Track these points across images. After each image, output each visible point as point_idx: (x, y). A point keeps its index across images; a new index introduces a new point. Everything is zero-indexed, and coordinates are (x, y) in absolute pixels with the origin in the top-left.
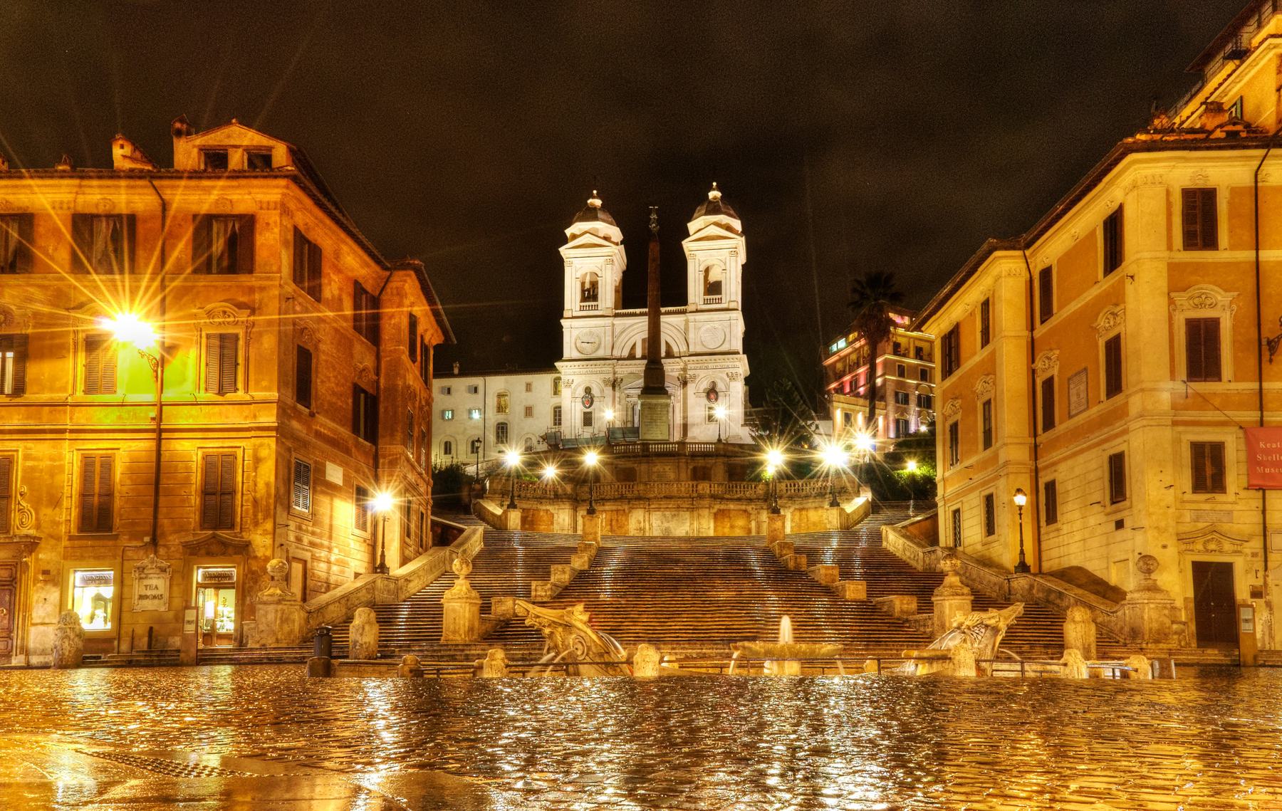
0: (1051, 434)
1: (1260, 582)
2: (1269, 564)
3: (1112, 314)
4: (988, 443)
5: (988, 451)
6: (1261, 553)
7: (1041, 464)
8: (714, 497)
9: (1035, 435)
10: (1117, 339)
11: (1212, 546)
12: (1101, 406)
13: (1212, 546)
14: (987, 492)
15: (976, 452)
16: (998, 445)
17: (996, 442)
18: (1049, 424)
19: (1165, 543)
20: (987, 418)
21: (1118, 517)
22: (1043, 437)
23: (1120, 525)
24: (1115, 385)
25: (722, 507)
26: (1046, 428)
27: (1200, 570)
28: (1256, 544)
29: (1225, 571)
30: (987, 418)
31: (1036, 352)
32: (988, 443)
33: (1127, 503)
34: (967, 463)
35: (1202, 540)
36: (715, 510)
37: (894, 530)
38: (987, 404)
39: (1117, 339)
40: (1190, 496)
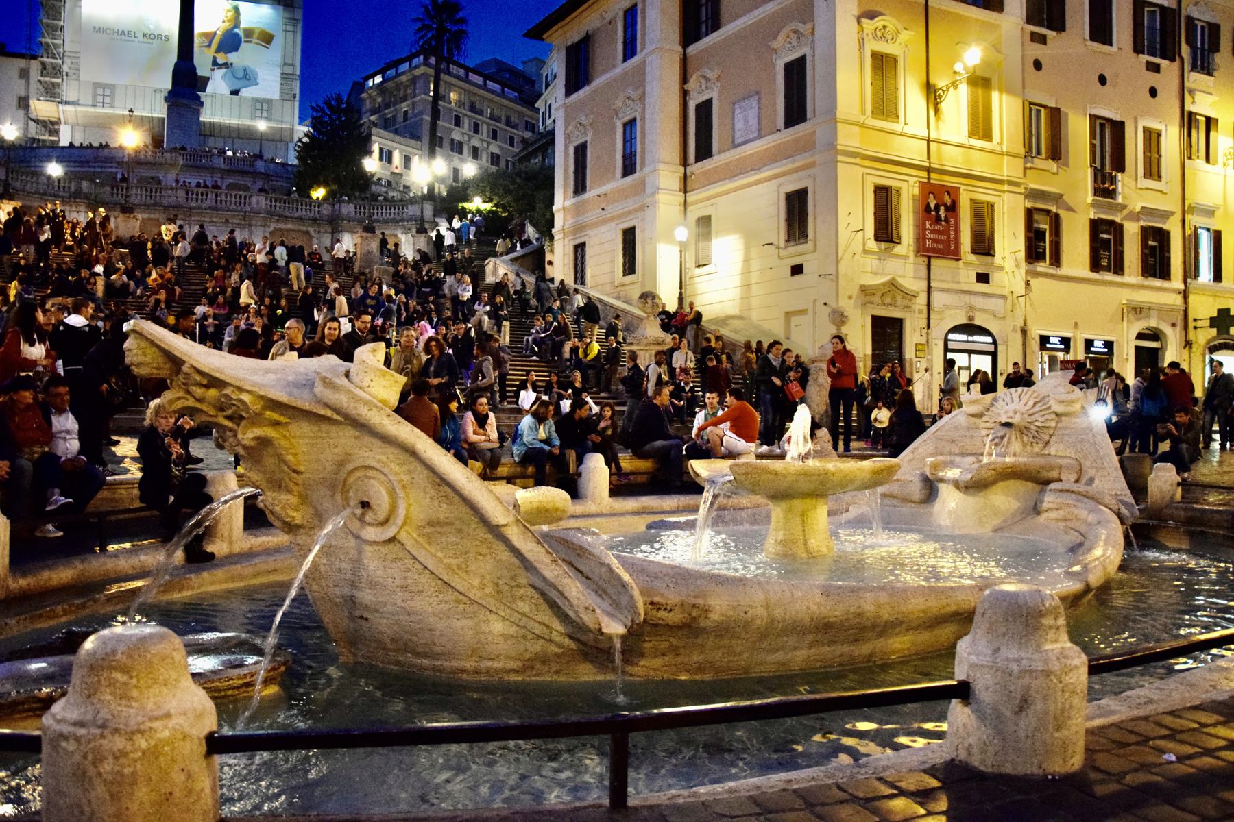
0: (707, 164)
1: (924, 341)
2: (932, 321)
3: (795, 32)
4: (629, 167)
5: (629, 179)
6: (925, 308)
7: (692, 197)
8: (271, 214)
9: (685, 163)
10: (802, 60)
11: (888, 300)
12: (777, 136)
13: (888, 300)
14: (627, 225)
15: (613, 178)
16: (646, 170)
17: (641, 169)
18: (704, 151)
19: (849, 293)
20: (629, 140)
21: (796, 261)
22: (697, 168)
23: (797, 270)
24: (796, 112)
25: (281, 226)
26: (698, 160)
27: (878, 323)
28: (922, 300)
29: (898, 324)
30: (629, 140)
31: (690, 70)
32: (629, 167)
33: (810, 245)
34: (600, 190)
35: (879, 294)
36: (272, 229)
37: (503, 261)
38: (630, 125)
39: (802, 60)
40: (872, 245)
